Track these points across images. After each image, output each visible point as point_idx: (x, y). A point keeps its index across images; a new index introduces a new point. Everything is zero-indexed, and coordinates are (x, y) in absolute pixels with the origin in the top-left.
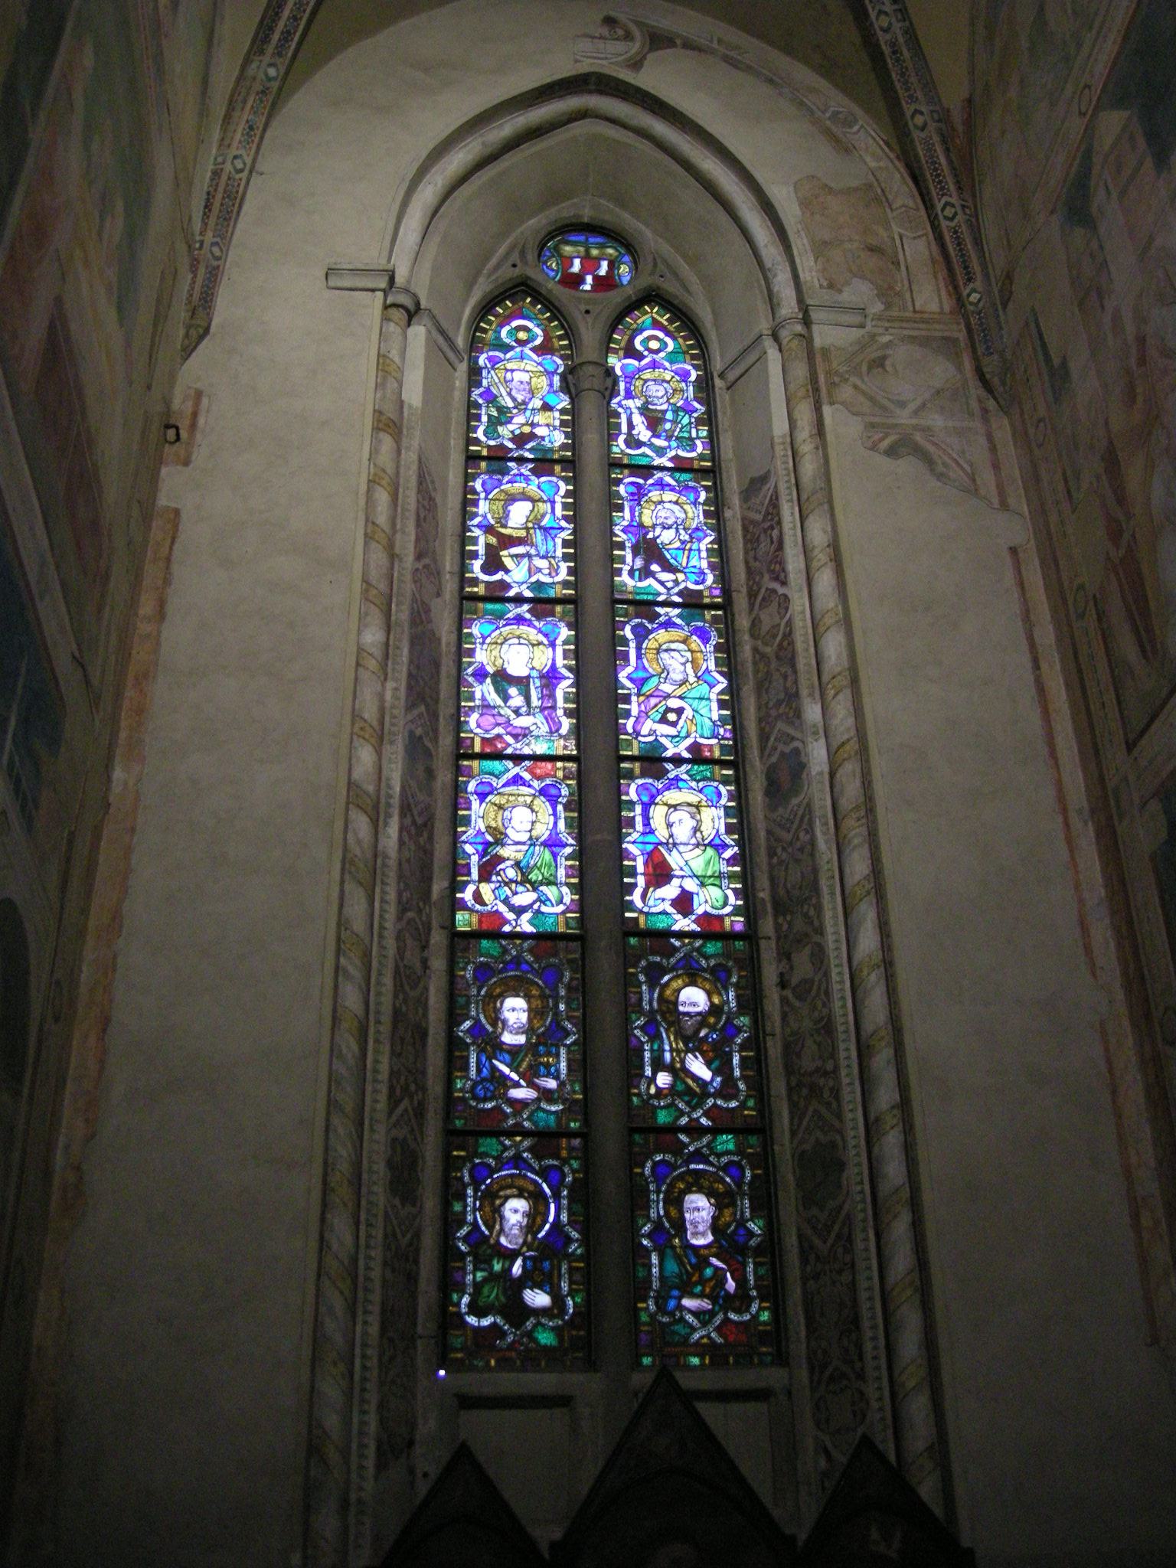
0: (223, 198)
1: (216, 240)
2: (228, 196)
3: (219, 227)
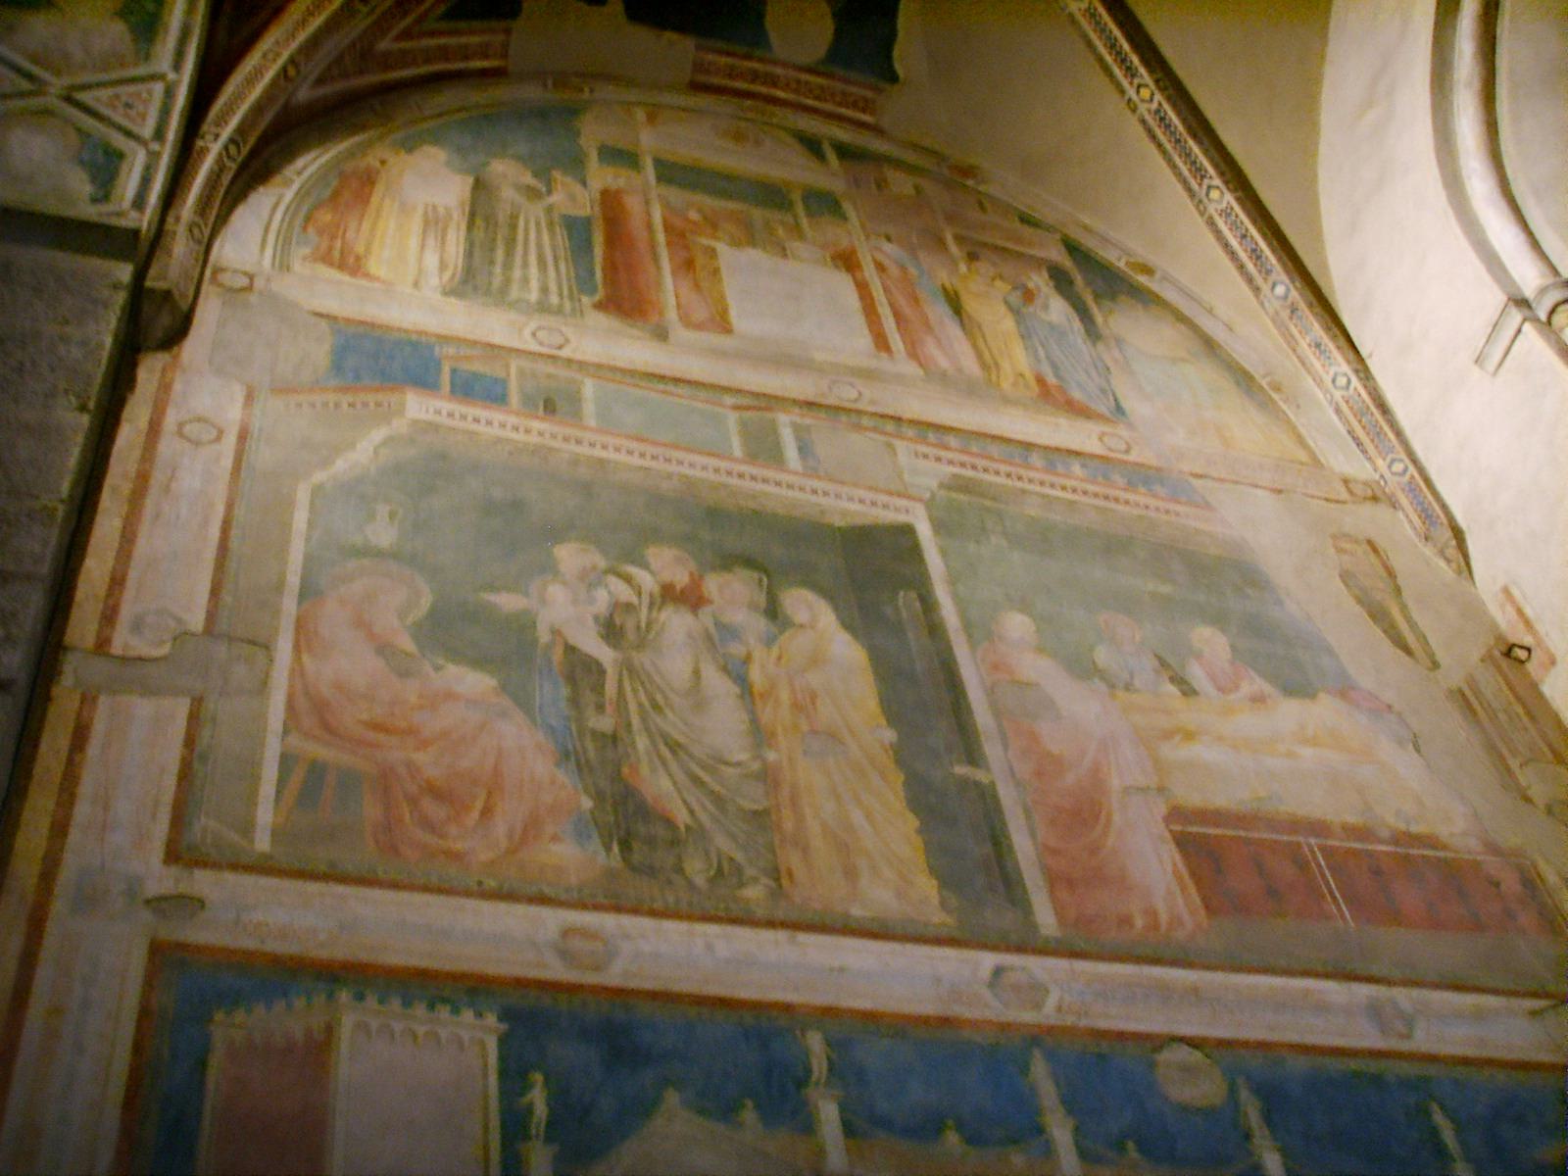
0: (1360, 421)
1: (1388, 460)
2: (1362, 415)
3: (1381, 446)
